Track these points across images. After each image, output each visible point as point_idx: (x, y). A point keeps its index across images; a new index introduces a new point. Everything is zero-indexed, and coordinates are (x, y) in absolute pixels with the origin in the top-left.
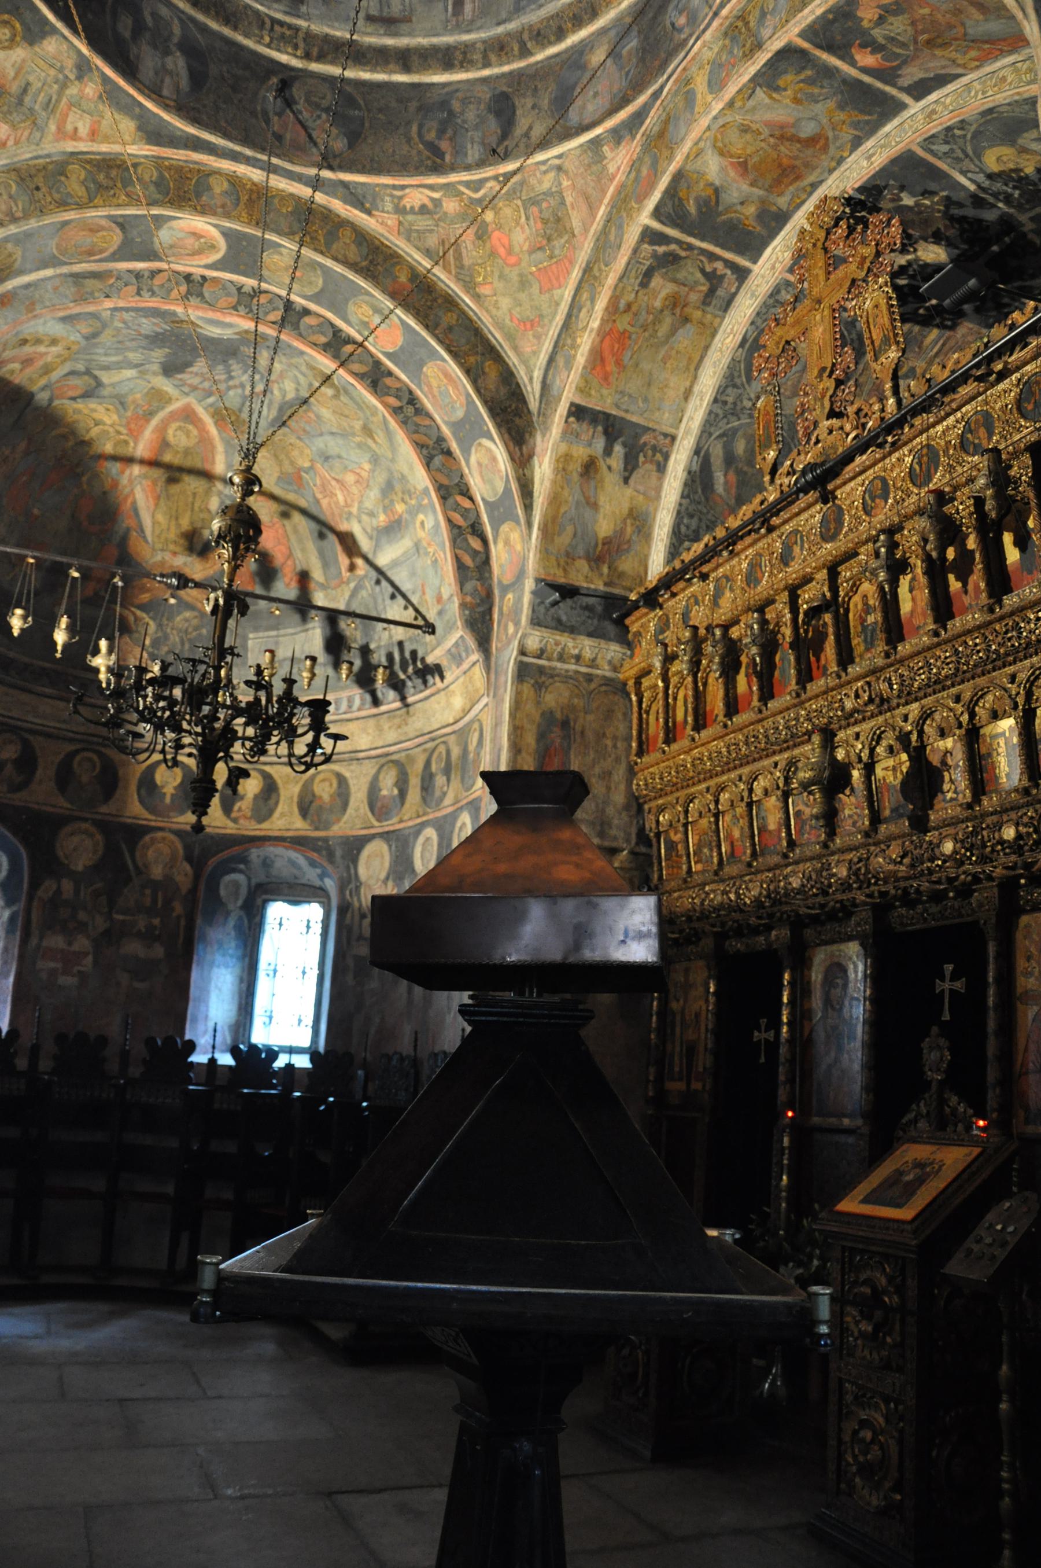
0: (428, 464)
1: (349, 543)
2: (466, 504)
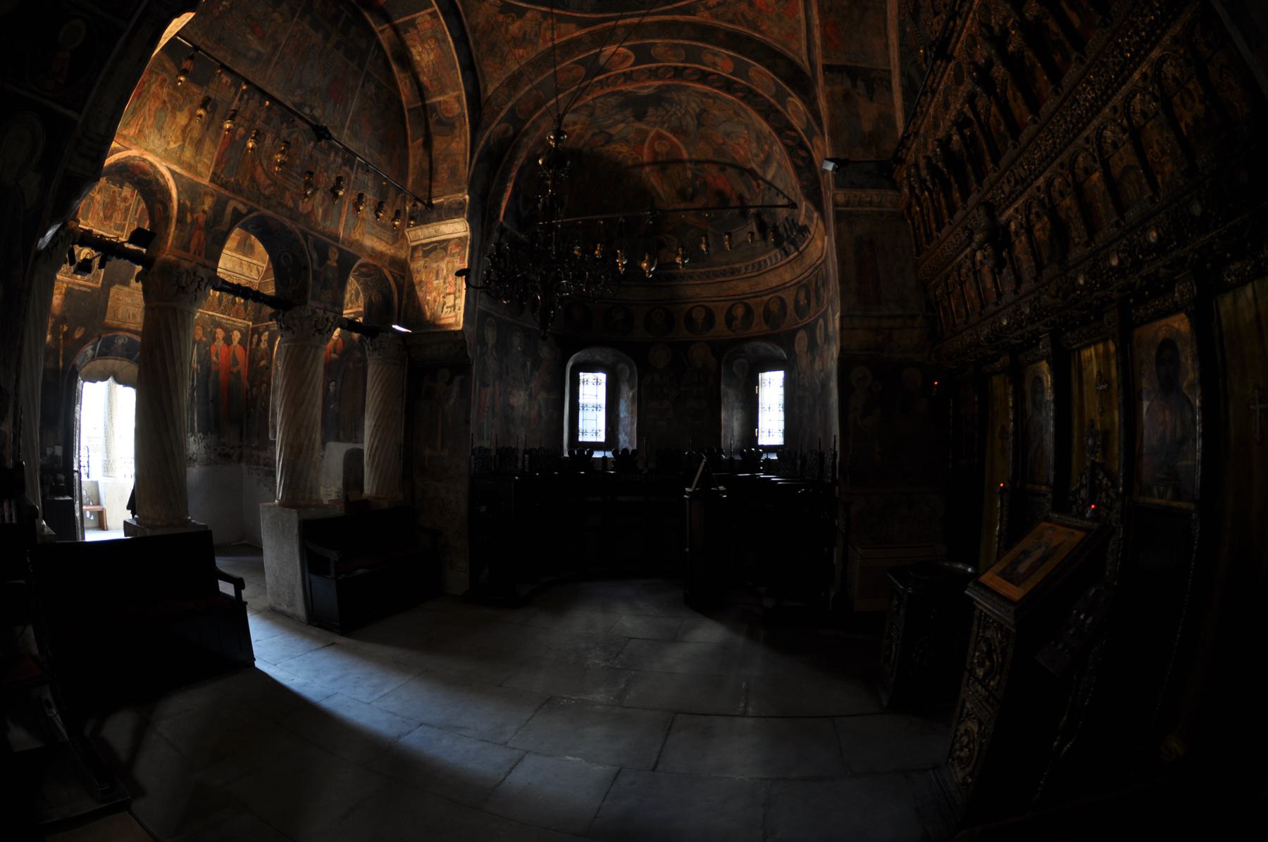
0: (766, 119)
1: (752, 172)
2: (793, 134)
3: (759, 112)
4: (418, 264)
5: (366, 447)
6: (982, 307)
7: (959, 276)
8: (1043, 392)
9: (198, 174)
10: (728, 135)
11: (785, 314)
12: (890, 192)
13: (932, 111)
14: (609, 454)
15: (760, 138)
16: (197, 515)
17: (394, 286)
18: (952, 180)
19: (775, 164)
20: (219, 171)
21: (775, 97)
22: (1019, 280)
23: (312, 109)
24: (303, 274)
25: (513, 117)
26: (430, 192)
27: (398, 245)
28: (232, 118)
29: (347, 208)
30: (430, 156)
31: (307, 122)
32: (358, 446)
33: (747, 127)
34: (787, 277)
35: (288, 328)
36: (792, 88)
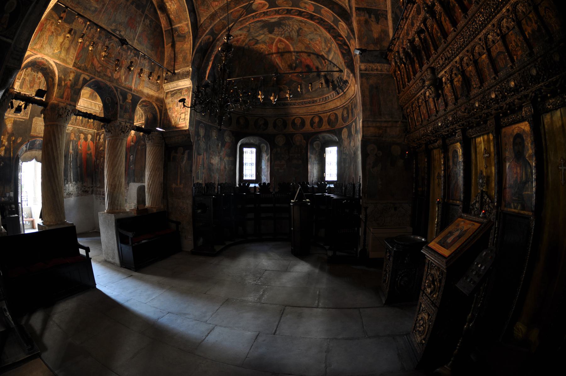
0: (329, 32)
1: (322, 57)
2: (341, 39)
3: (326, 29)
4: (168, 101)
5: (146, 184)
6: (429, 117)
7: (418, 103)
8: (458, 157)
9: (67, 63)
10: (312, 40)
11: (338, 120)
12: (386, 65)
13: (406, 27)
14: (257, 185)
15: (326, 41)
16: (71, 218)
17: (158, 110)
18: (415, 58)
19: (333, 53)
20: (77, 61)
21: (333, 22)
22: (446, 105)
23: (120, 32)
24: (116, 107)
25: (212, 33)
26: (174, 67)
27: (160, 92)
28: (82, 37)
29: (136, 76)
30: (174, 51)
31: (117, 37)
32: (143, 184)
33: (320, 36)
34: (338, 104)
35: (109, 131)
36: (341, 18)
